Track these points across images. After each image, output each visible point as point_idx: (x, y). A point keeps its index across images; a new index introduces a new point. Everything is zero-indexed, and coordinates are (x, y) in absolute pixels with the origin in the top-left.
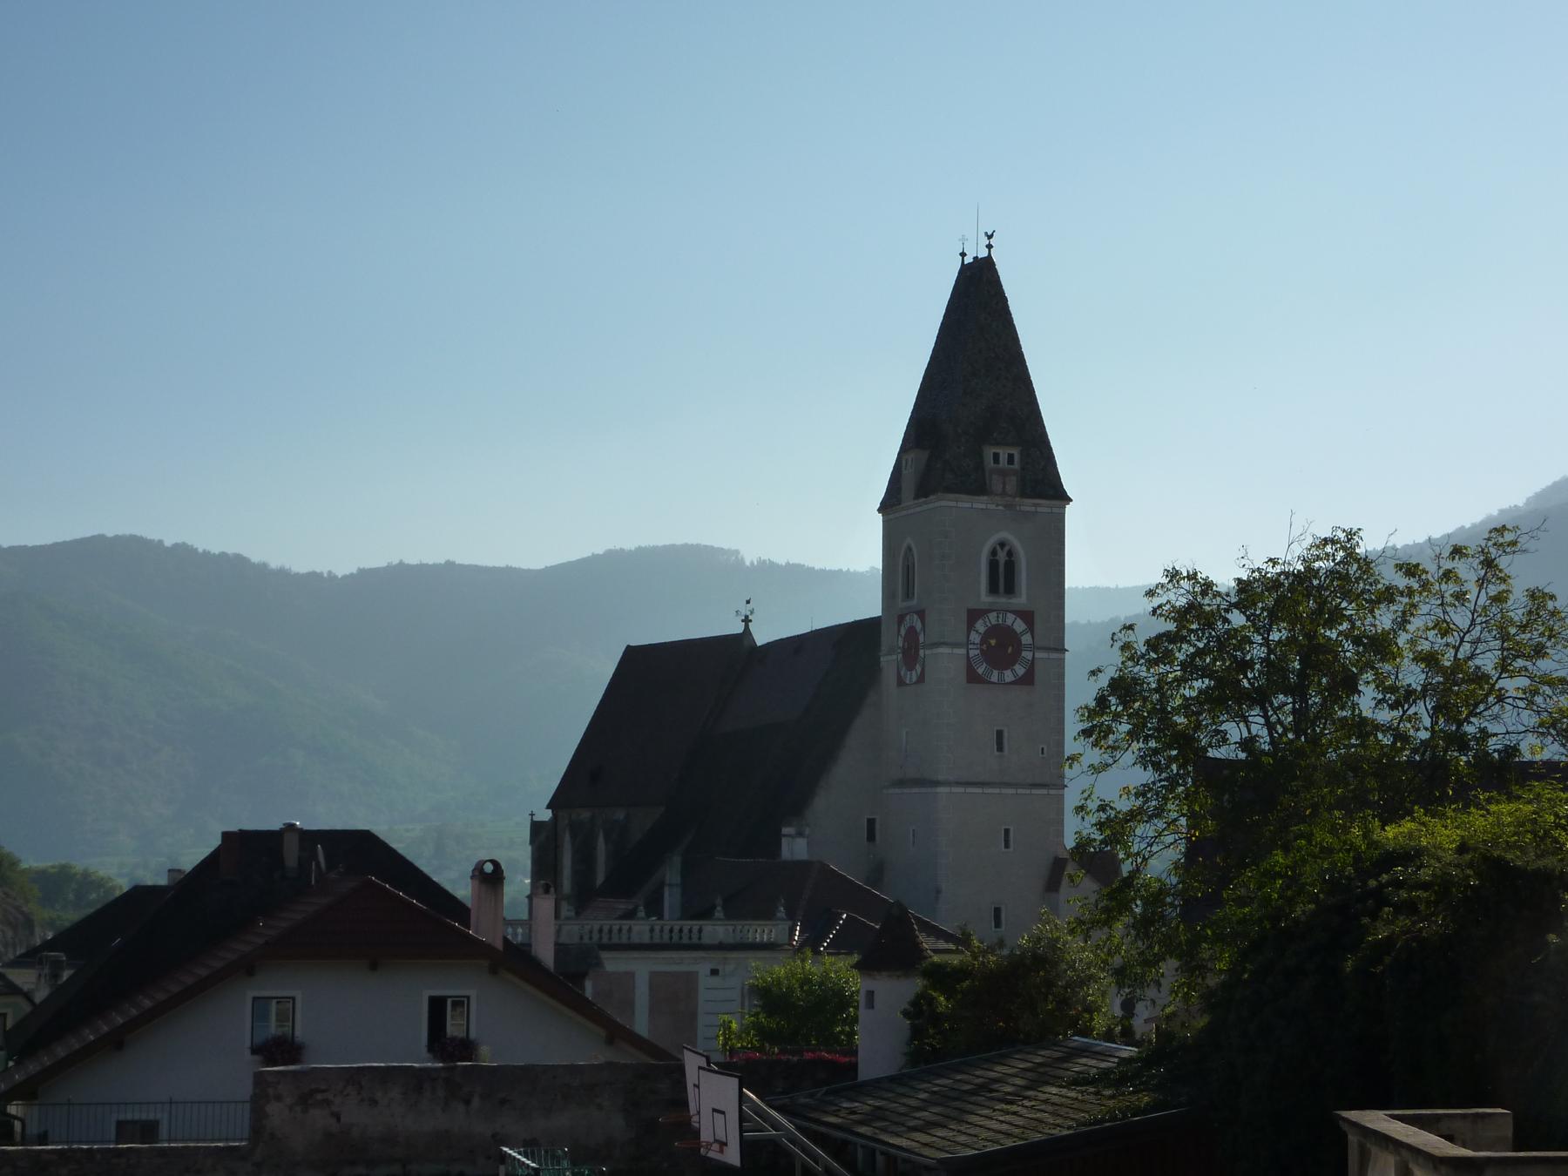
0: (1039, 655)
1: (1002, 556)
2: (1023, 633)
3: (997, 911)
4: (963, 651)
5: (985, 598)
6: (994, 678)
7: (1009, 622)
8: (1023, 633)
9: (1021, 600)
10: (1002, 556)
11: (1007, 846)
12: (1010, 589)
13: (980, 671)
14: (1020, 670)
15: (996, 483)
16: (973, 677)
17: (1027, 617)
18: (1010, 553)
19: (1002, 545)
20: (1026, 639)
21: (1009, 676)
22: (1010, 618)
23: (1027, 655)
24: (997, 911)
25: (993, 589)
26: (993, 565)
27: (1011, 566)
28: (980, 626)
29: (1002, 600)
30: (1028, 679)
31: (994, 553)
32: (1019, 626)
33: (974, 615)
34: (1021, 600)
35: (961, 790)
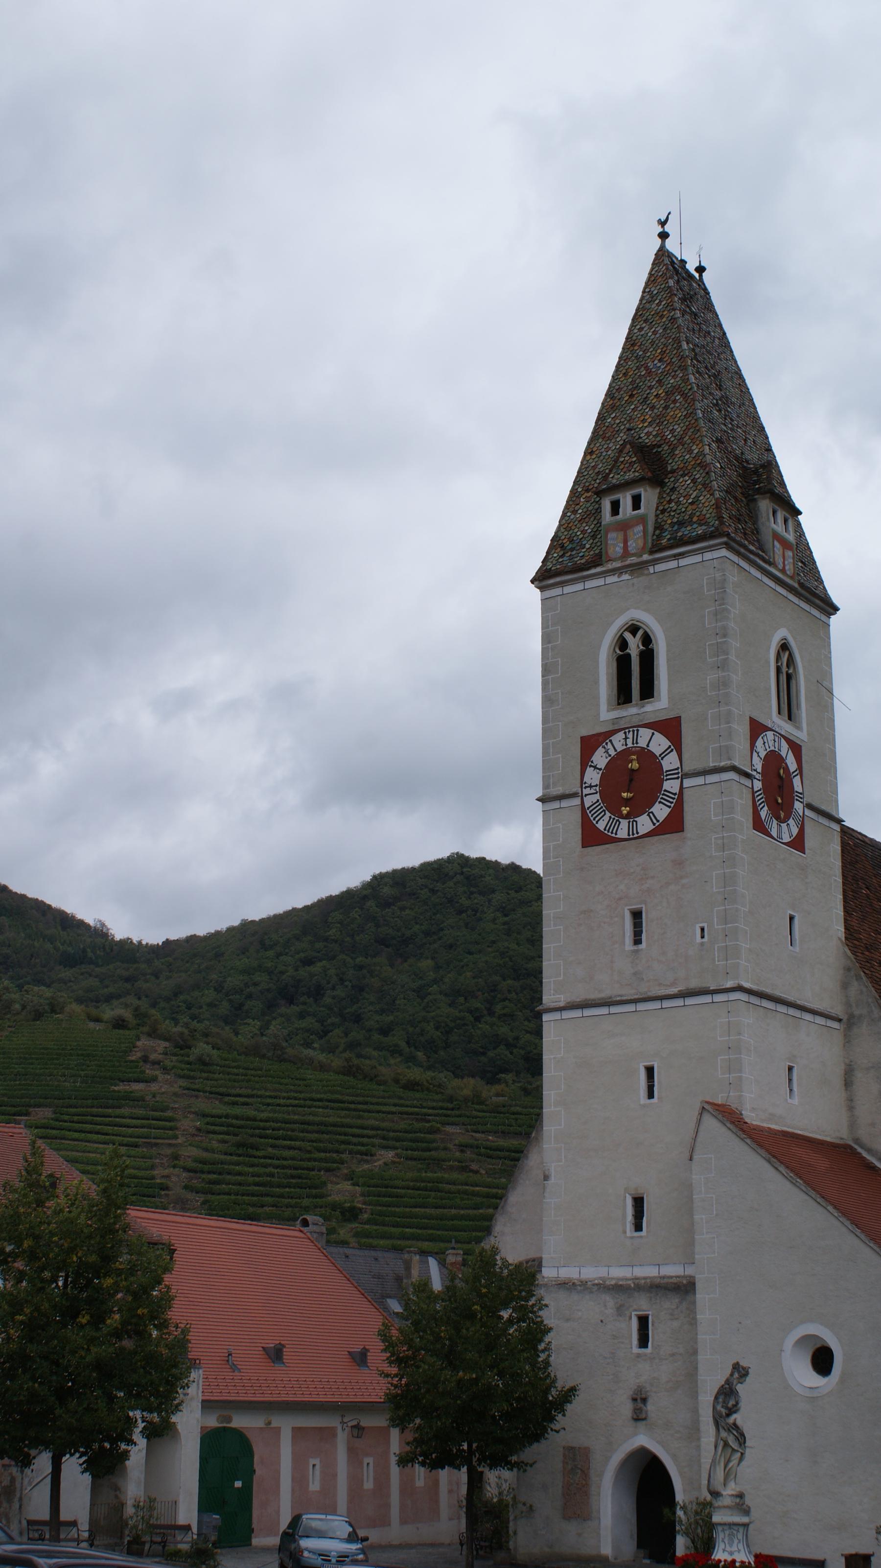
0: (687, 783)
1: (634, 645)
2: (664, 754)
3: (639, 1202)
4: (577, 801)
5: (605, 713)
6: (622, 833)
7: (642, 743)
8: (664, 754)
9: (660, 705)
10: (634, 645)
11: (651, 1095)
12: (648, 691)
13: (601, 826)
14: (661, 811)
15: (614, 545)
16: (592, 837)
17: (670, 728)
18: (647, 640)
19: (634, 629)
20: (670, 762)
21: (644, 824)
22: (645, 733)
23: (671, 786)
24: (639, 1202)
25: (623, 696)
26: (623, 663)
27: (648, 657)
28: (600, 758)
29: (631, 711)
30: (674, 824)
31: (623, 644)
32: (659, 743)
33: (589, 745)
34: (660, 705)
35: (577, 1013)
